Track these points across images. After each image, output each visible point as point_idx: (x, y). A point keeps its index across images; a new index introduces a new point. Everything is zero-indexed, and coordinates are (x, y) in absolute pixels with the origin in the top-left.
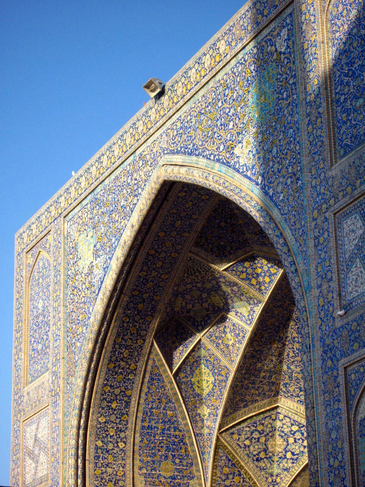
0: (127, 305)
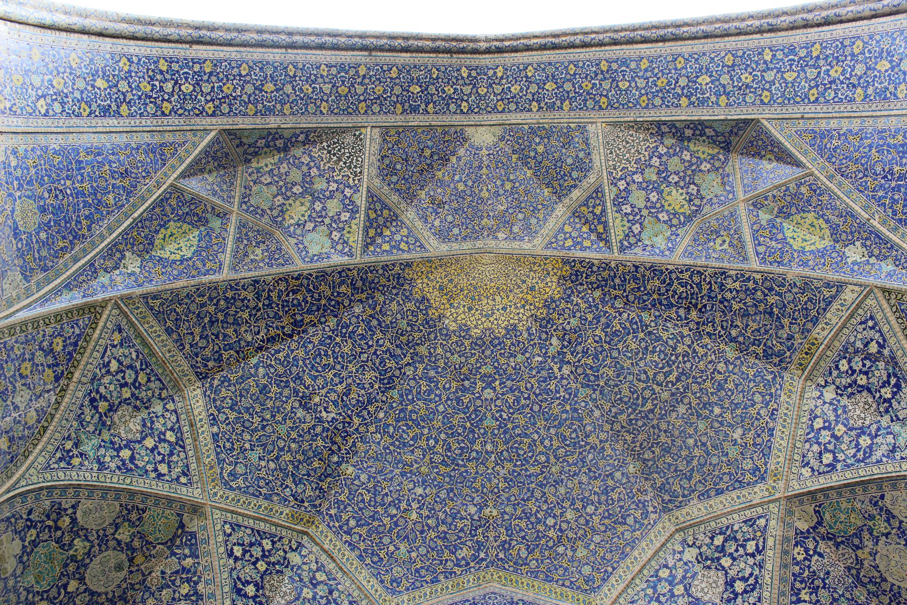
0: (268, 63)
